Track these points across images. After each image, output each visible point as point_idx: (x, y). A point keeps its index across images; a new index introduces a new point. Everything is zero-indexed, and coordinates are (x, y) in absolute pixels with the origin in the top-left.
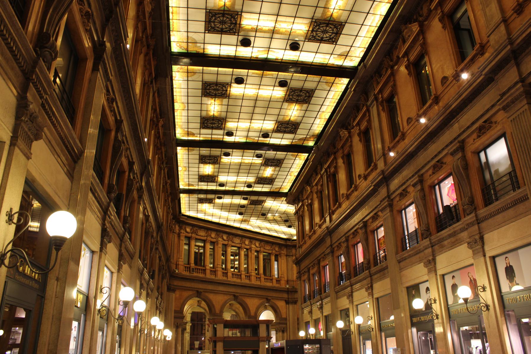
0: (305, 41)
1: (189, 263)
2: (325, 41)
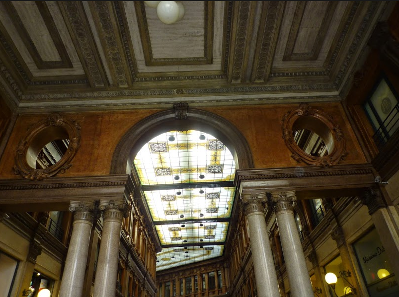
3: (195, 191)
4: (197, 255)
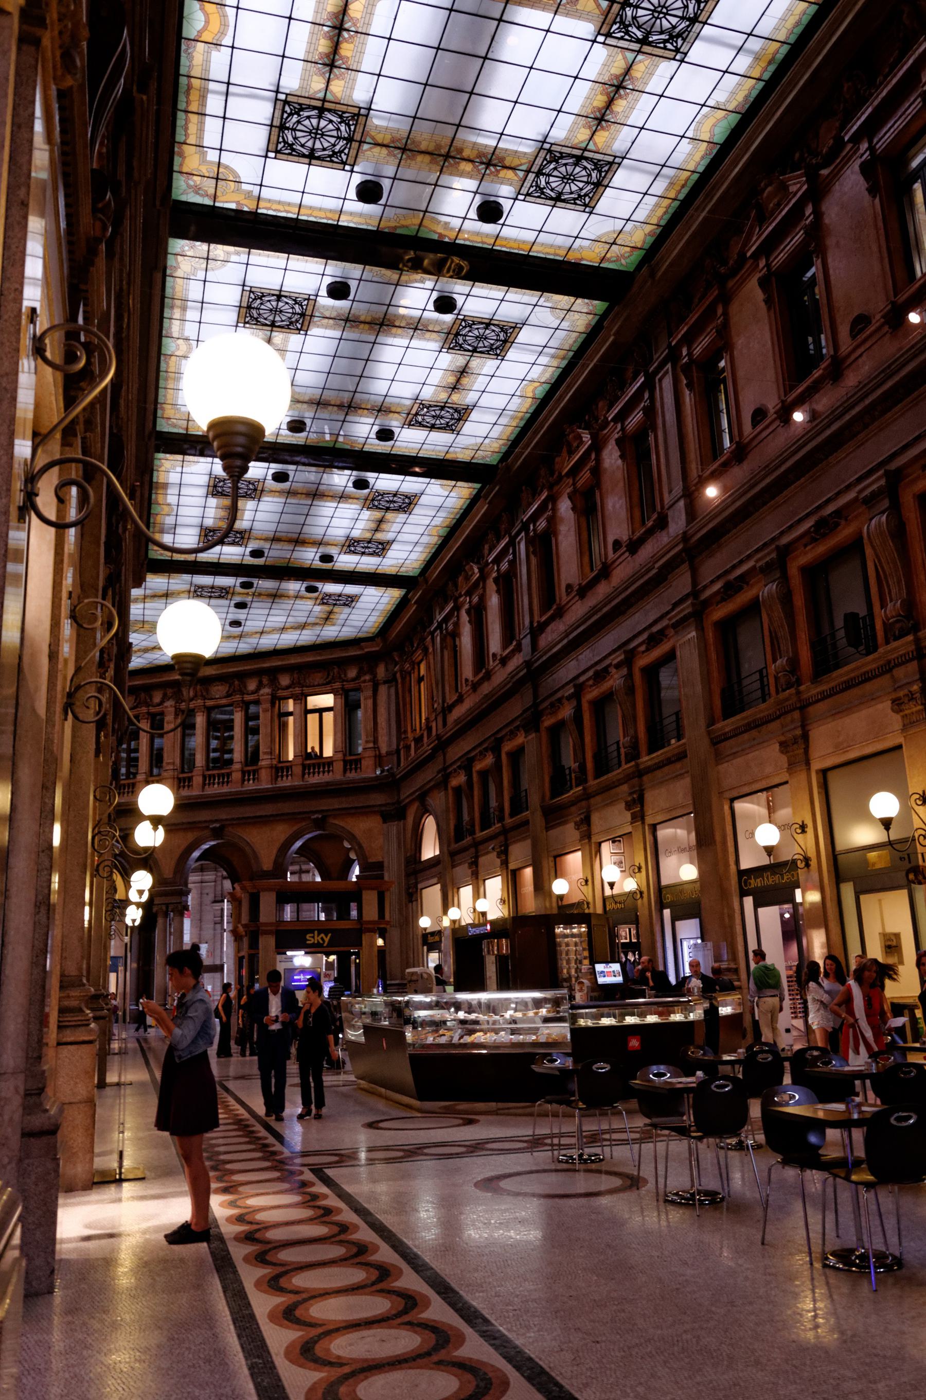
0: (516, 199)
2: (564, 201)
4: (284, 622)
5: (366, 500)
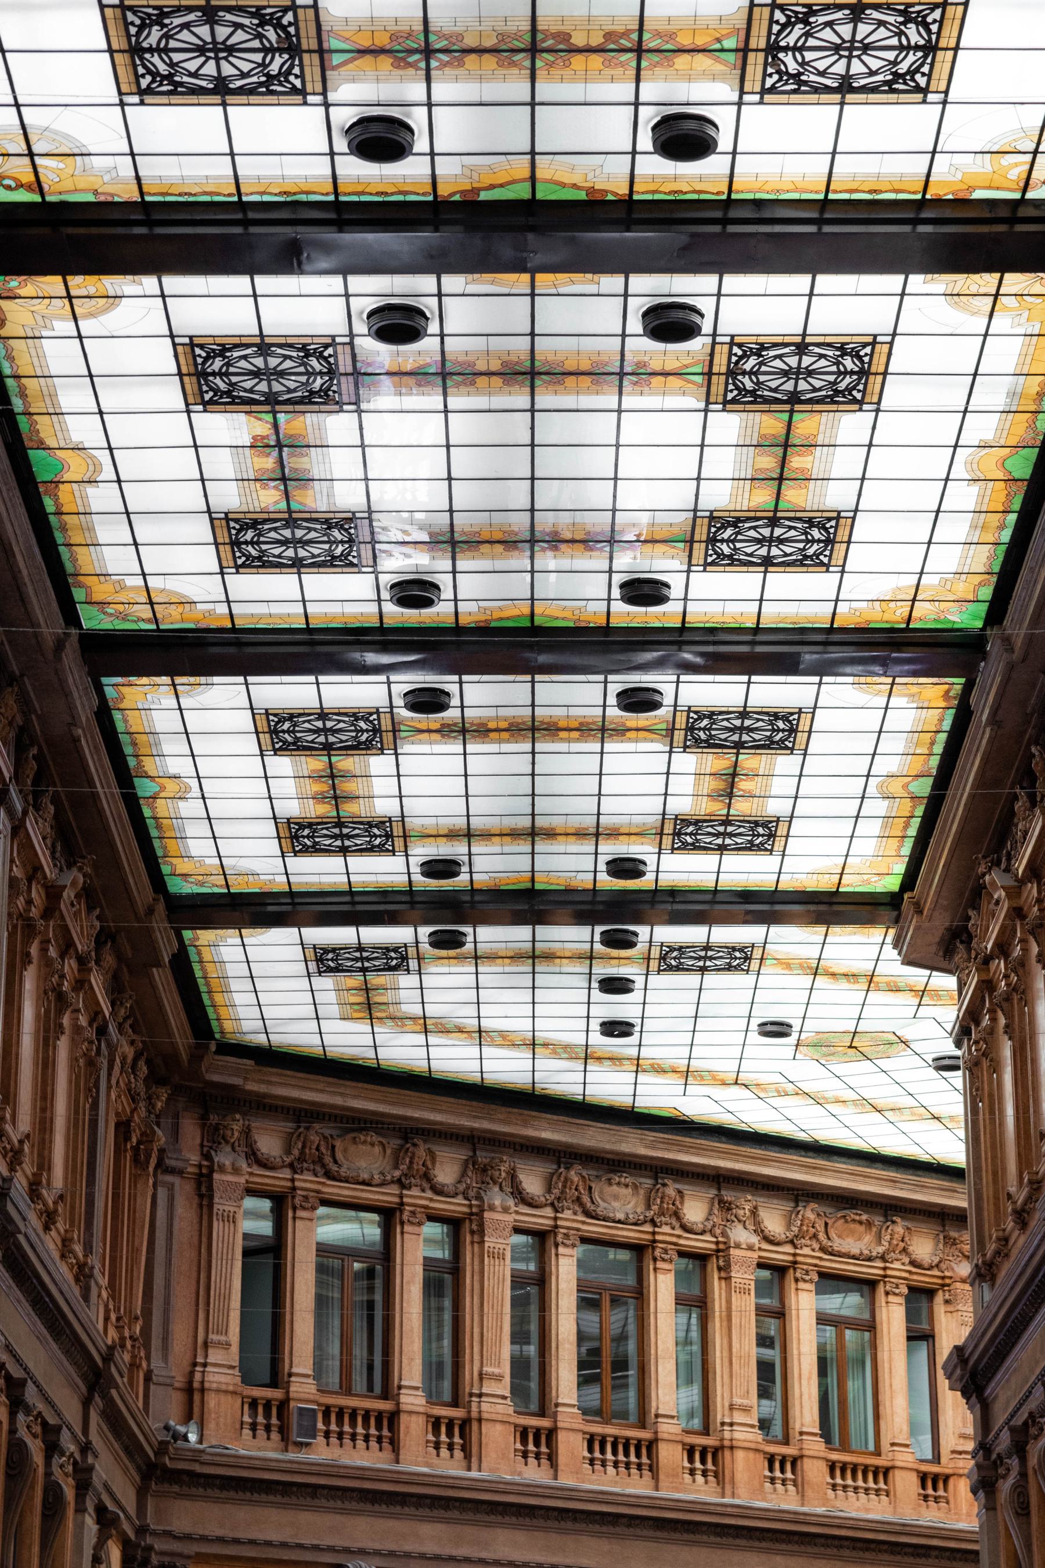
1: (277, 1377)
3: (591, 311)
5: (671, 731)
